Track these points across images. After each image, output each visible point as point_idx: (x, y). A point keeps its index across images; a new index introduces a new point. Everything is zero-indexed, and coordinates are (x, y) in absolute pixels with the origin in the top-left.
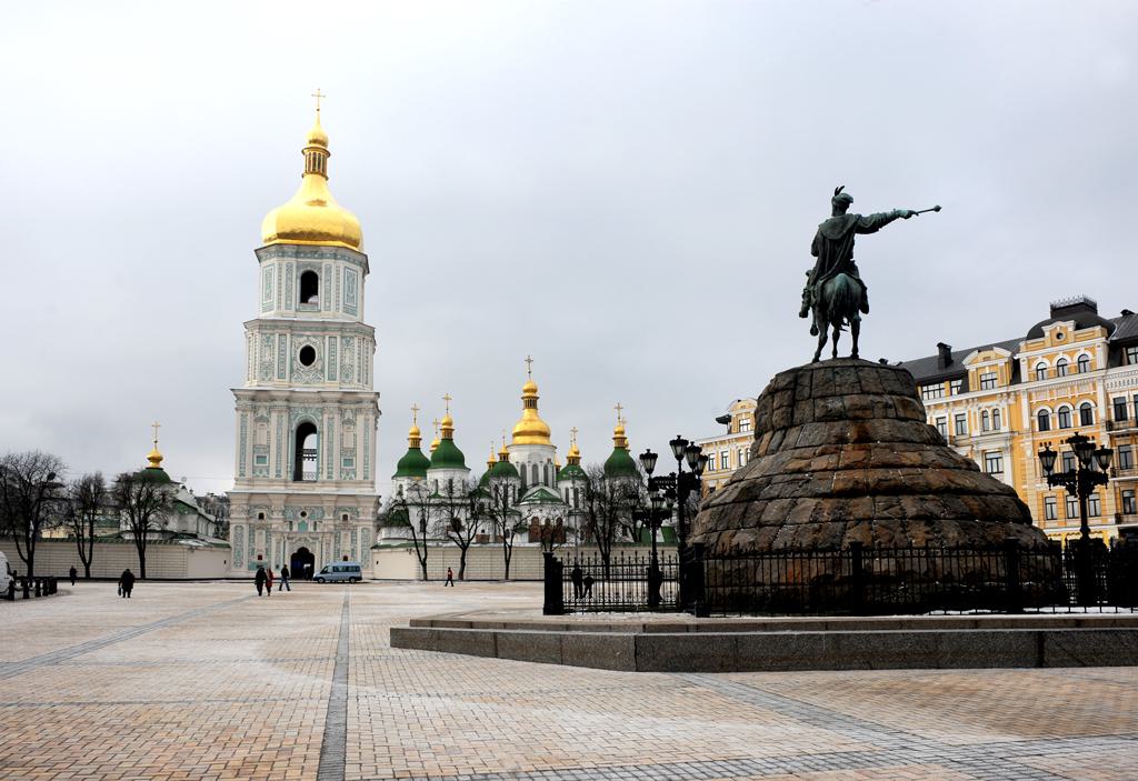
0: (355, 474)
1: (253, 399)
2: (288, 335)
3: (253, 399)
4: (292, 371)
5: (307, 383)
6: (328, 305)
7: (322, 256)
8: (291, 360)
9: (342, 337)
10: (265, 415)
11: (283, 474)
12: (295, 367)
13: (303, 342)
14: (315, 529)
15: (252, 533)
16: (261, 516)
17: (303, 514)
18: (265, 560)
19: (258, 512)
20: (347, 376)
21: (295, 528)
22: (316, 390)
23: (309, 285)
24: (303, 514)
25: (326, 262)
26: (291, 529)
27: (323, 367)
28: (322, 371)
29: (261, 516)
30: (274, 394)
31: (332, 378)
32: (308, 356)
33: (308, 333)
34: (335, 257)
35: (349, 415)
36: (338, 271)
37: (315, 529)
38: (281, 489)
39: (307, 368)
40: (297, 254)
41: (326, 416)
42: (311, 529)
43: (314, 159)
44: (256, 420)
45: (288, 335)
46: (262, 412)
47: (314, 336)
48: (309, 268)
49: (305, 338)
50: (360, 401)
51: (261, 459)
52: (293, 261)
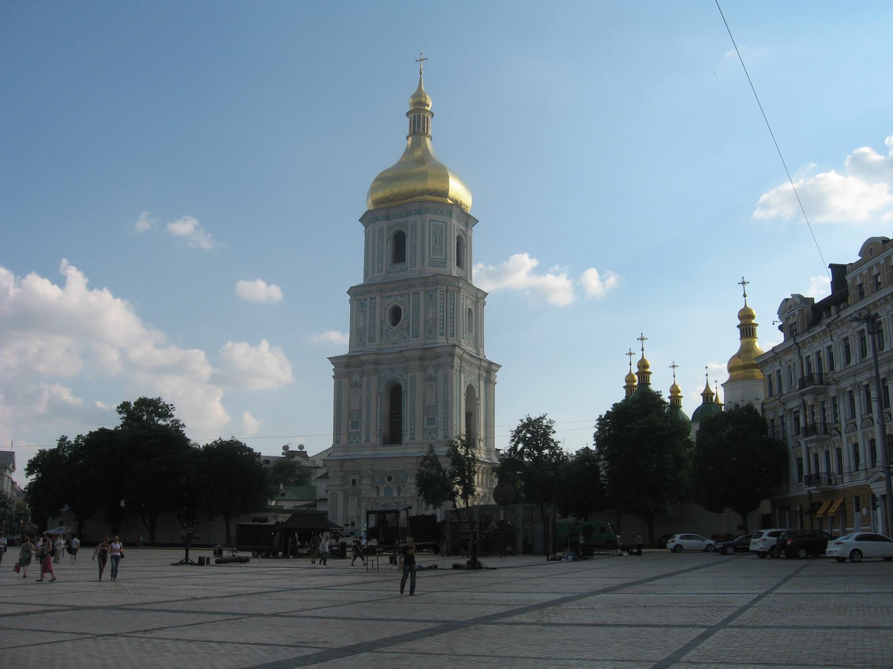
0: (436, 433)
1: (347, 366)
2: (378, 298)
3: (347, 366)
4: (382, 334)
5: (395, 343)
6: (419, 263)
7: (408, 214)
8: (381, 322)
9: (426, 292)
10: (358, 380)
11: (373, 438)
12: (384, 329)
13: (391, 302)
14: (399, 494)
15: (346, 498)
16: (354, 482)
17: (390, 479)
18: (356, 527)
19: (351, 478)
20: (430, 331)
21: (382, 493)
22: (397, 350)
23: (399, 241)
24: (390, 479)
25: (411, 219)
26: (378, 494)
27: (409, 325)
28: (408, 329)
29: (354, 482)
30: (363, 358)
31: (416, 335)
32: (396, 315)
33: (396, 293)
34: (420, 212)
35: (431, 372)
36: (423, 225)
37: (399, 494)
38: (369, 453)
39: (395, 328)
40: (387, 218)
41: (409, 375)
42: (395, 494)
43: (414, 121)
44: (351, 387)
45: (378, 298)
46: (356, 378)
47: (401, 296)
48: (398, 228)
49: (393, 298)
50: (439, 356)
51: (355, 424)
52: (384, 224)
